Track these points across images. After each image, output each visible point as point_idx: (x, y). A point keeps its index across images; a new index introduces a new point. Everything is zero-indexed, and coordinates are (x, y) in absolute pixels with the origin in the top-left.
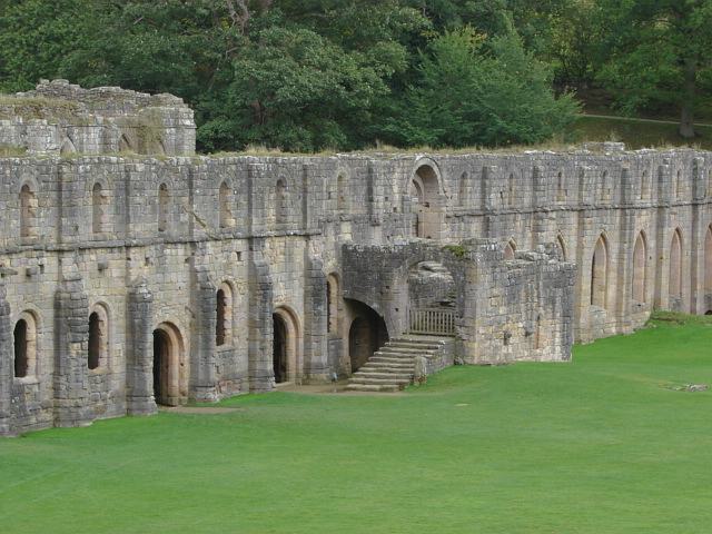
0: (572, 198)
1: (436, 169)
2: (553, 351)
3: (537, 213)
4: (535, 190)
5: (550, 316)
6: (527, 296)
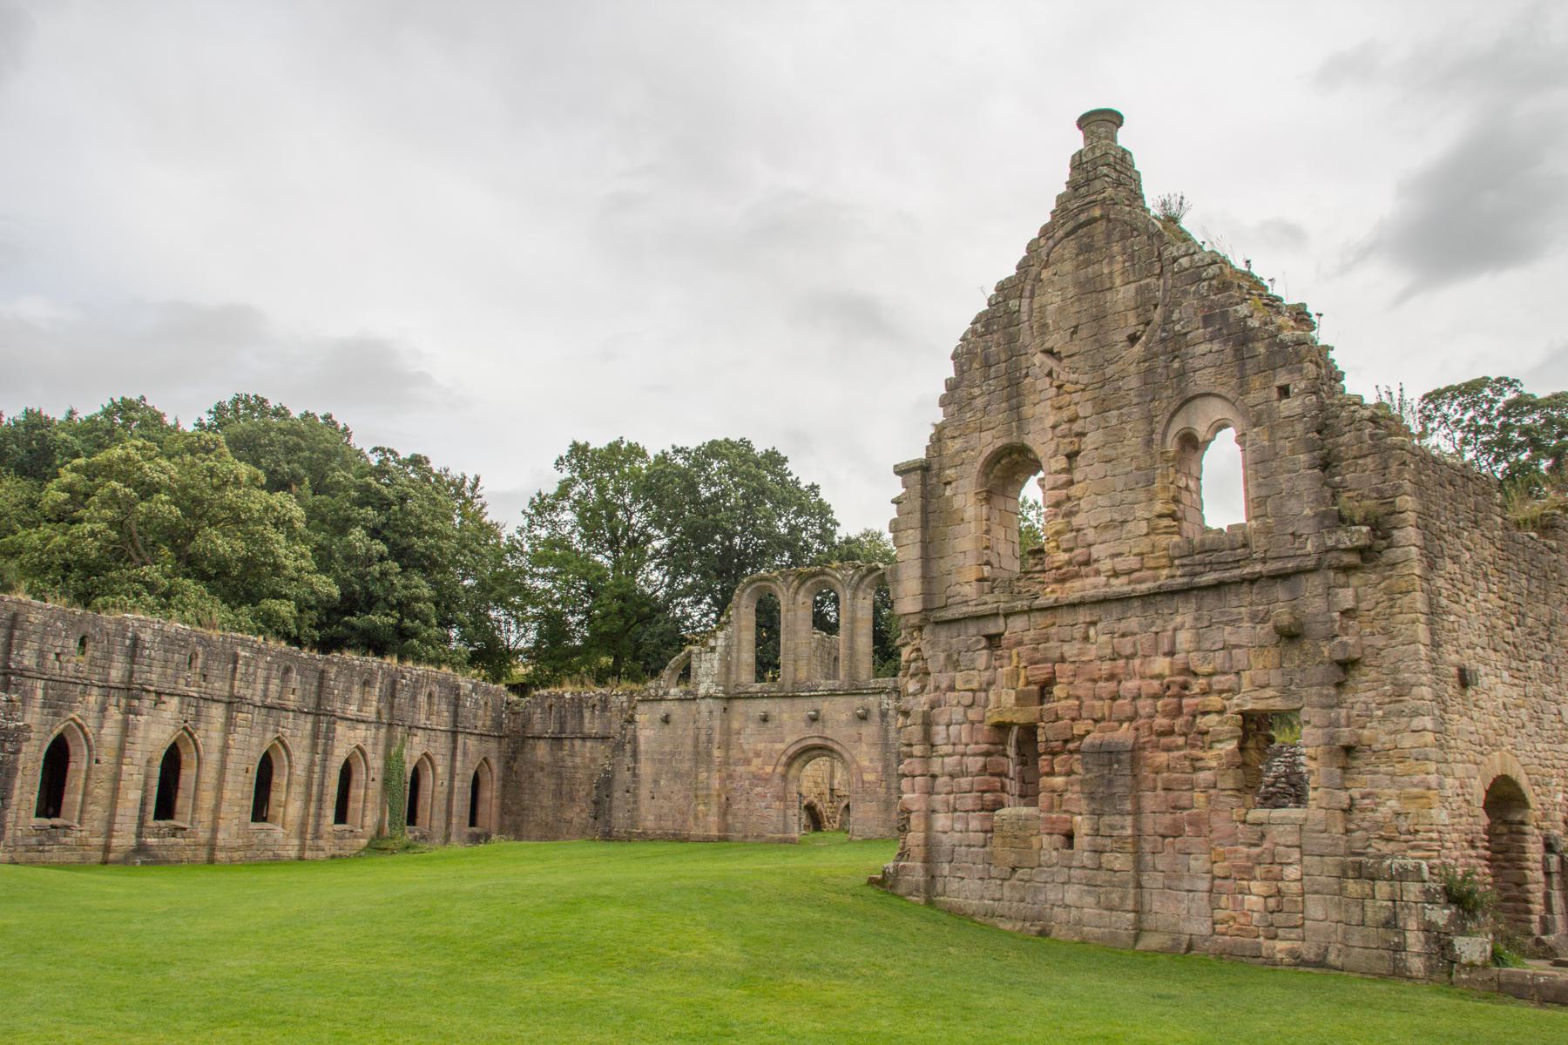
3: (131, 690)
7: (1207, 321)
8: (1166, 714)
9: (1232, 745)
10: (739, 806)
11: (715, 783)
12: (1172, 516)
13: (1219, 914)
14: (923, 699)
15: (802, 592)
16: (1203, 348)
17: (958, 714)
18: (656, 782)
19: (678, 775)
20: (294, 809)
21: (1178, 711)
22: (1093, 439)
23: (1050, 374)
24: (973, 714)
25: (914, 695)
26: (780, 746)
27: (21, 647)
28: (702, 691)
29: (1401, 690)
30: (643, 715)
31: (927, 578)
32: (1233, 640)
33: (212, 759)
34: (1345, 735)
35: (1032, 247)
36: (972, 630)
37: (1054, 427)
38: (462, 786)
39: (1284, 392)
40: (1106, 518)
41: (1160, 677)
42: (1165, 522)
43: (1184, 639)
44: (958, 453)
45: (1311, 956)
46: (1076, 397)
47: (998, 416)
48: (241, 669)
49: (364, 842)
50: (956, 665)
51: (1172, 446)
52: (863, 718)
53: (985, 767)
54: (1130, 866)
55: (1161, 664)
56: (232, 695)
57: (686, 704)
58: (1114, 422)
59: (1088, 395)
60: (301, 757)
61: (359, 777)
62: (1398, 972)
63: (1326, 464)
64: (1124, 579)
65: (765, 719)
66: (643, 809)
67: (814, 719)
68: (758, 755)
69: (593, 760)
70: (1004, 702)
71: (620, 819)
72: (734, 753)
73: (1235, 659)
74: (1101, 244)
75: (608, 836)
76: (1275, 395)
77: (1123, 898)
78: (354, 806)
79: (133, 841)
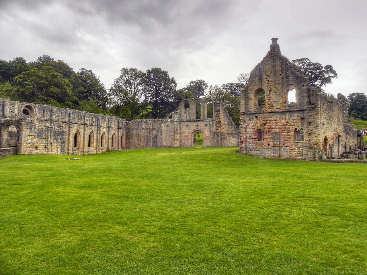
0: (82, 121)
1: (33, 107)
2: (58, 153)
4: (69, 118)
5: (56, 143)
6: (46, 137)
7: (292, 74)
8: (284, 128)
9: (293, 132)
10: (183, 141)
11: (179, 137)
12: (285, 101)
13: (291, 154)
15: (194, 103)
16: (292, 78)
17: (251, 127)
18: (166, 137)
19: (170, 136)
20: (95, 144)
21: (286, 128)
22: (274, 89)
23: (267, 78)
24: (253, 128)
25: (242, 124)
26: (191, 130)
27: (53, 116)
28: (175, 120)
29: (317, 126)
30: (163, 125)
31: (246, 107)
32: (294, 119)
33: (82, 135)
34: (310, 131)
35: (264, 59)
36: (253, 115)
38: (120, 138)
39: (303, 85)
40: (275, 101)
41: (283, 123)
42: (284, 102)
43: (287, 118)
44: (251, 89)
45: (303, 159)
46: (271, 82)
47: (258, 83)
48: (86, 118)
49: (106, 150)
50: (250, 120)
52: (206, 125)
54: (279, 148)
55: (283, 121)
56: (85, 123)
57: (172, 123)
58: (277, 87)
59: (273, 82)
60: (95, 134)
61: (104, 138)
62: (315, 160)
64: (278, 109)
65: (187, 126)
66: (163, 142)
67: (197, 126)
68: (186, 132)
69: (145, 133)
70: (258, 126)
71: (159, 144)
72: (182, 132)
73: (295, 120)
74: (276, 60)
75: (157, 147)
76: (302, 86)
77: (277, 153)
78: (103, 143)
79: (72, 151)
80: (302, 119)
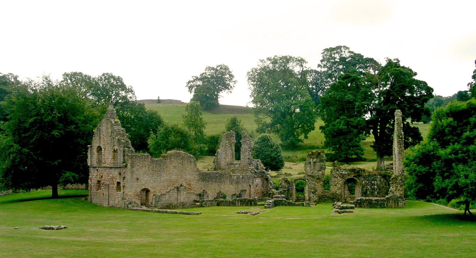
14: (91, 176)
24: (95, 179)
37: (103, 145)
42: (112, 159)
51: (113, 151)
53: (96, 185)
55: (111, 175)
62: (125, 208)
63: (124, 156)
80: (120, 174)
